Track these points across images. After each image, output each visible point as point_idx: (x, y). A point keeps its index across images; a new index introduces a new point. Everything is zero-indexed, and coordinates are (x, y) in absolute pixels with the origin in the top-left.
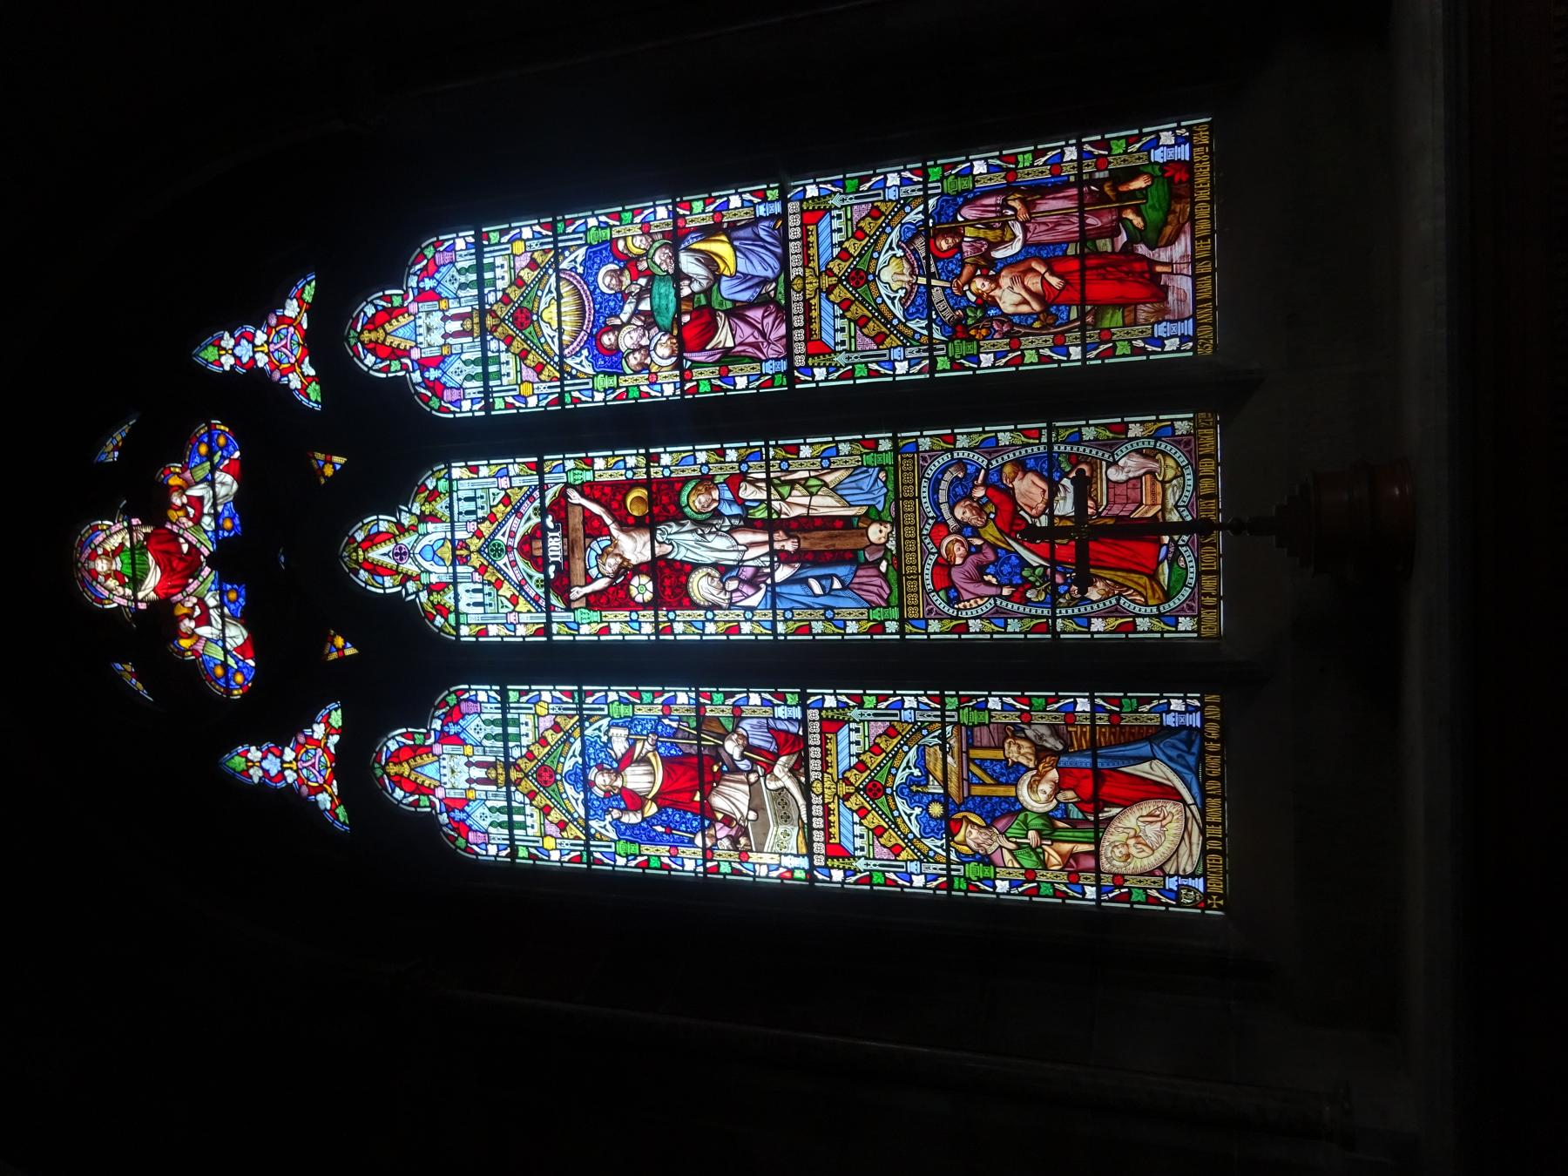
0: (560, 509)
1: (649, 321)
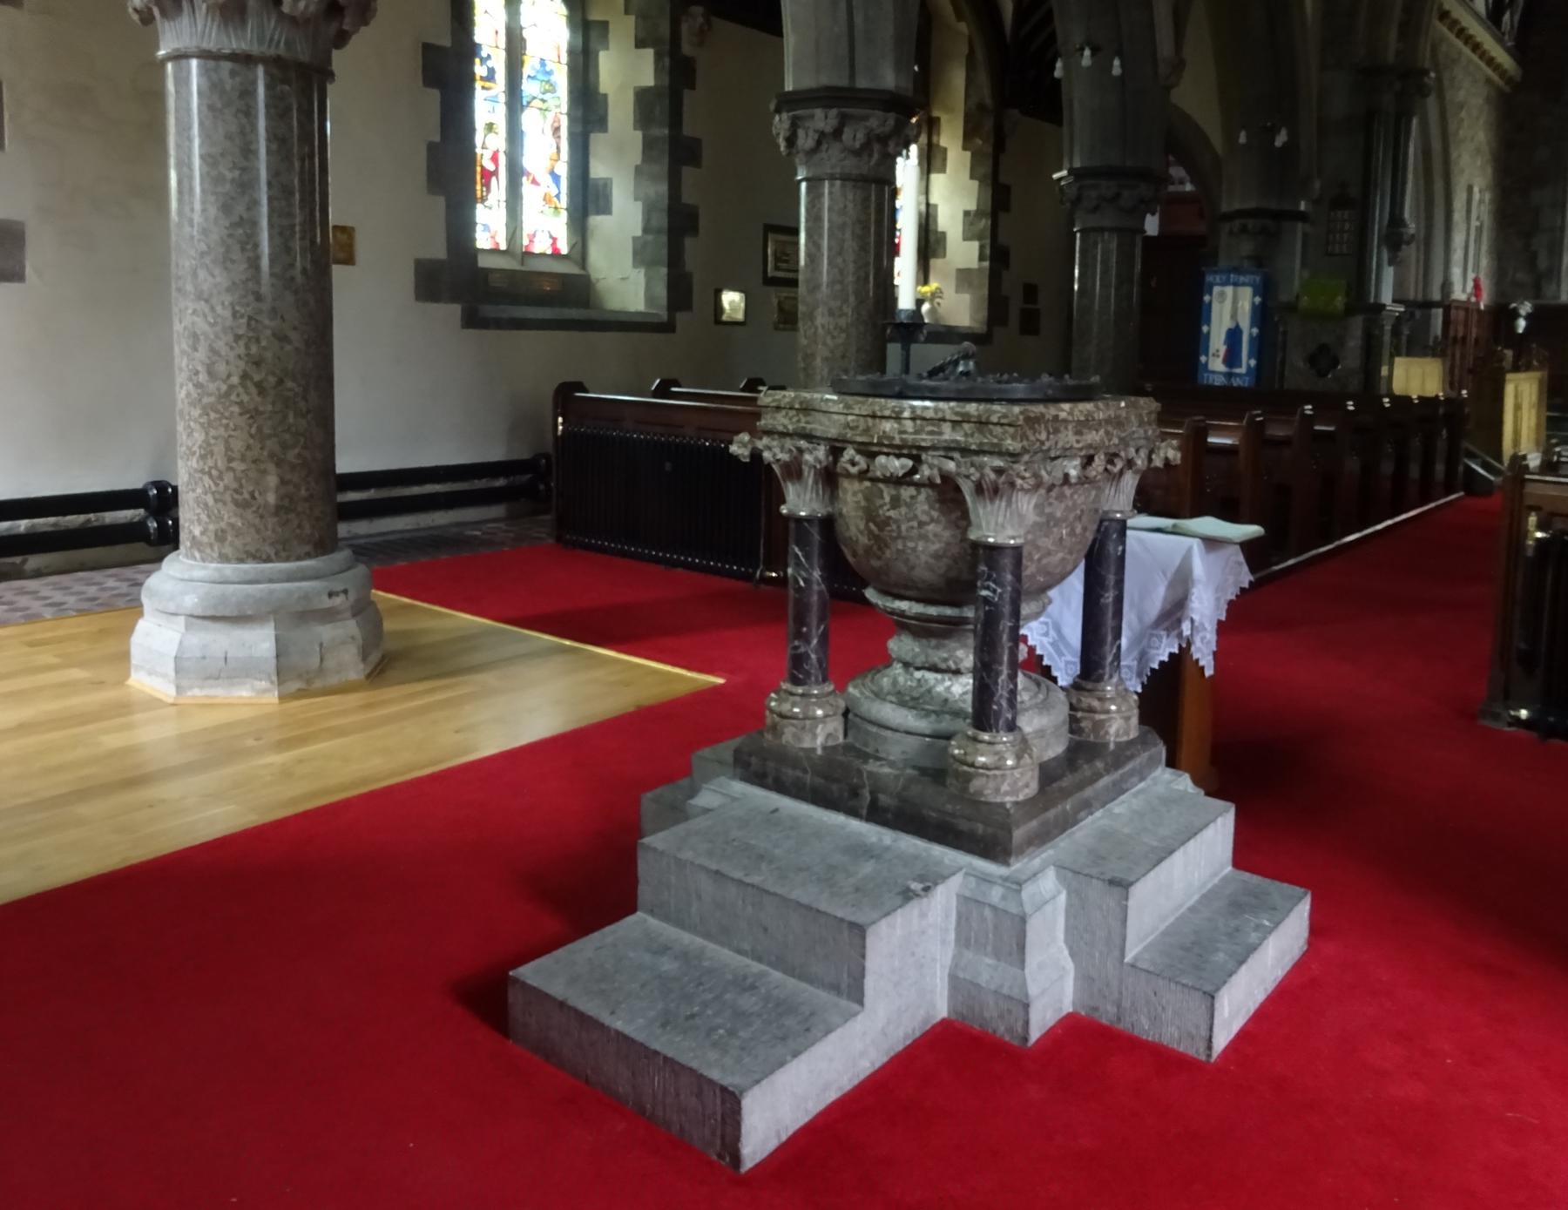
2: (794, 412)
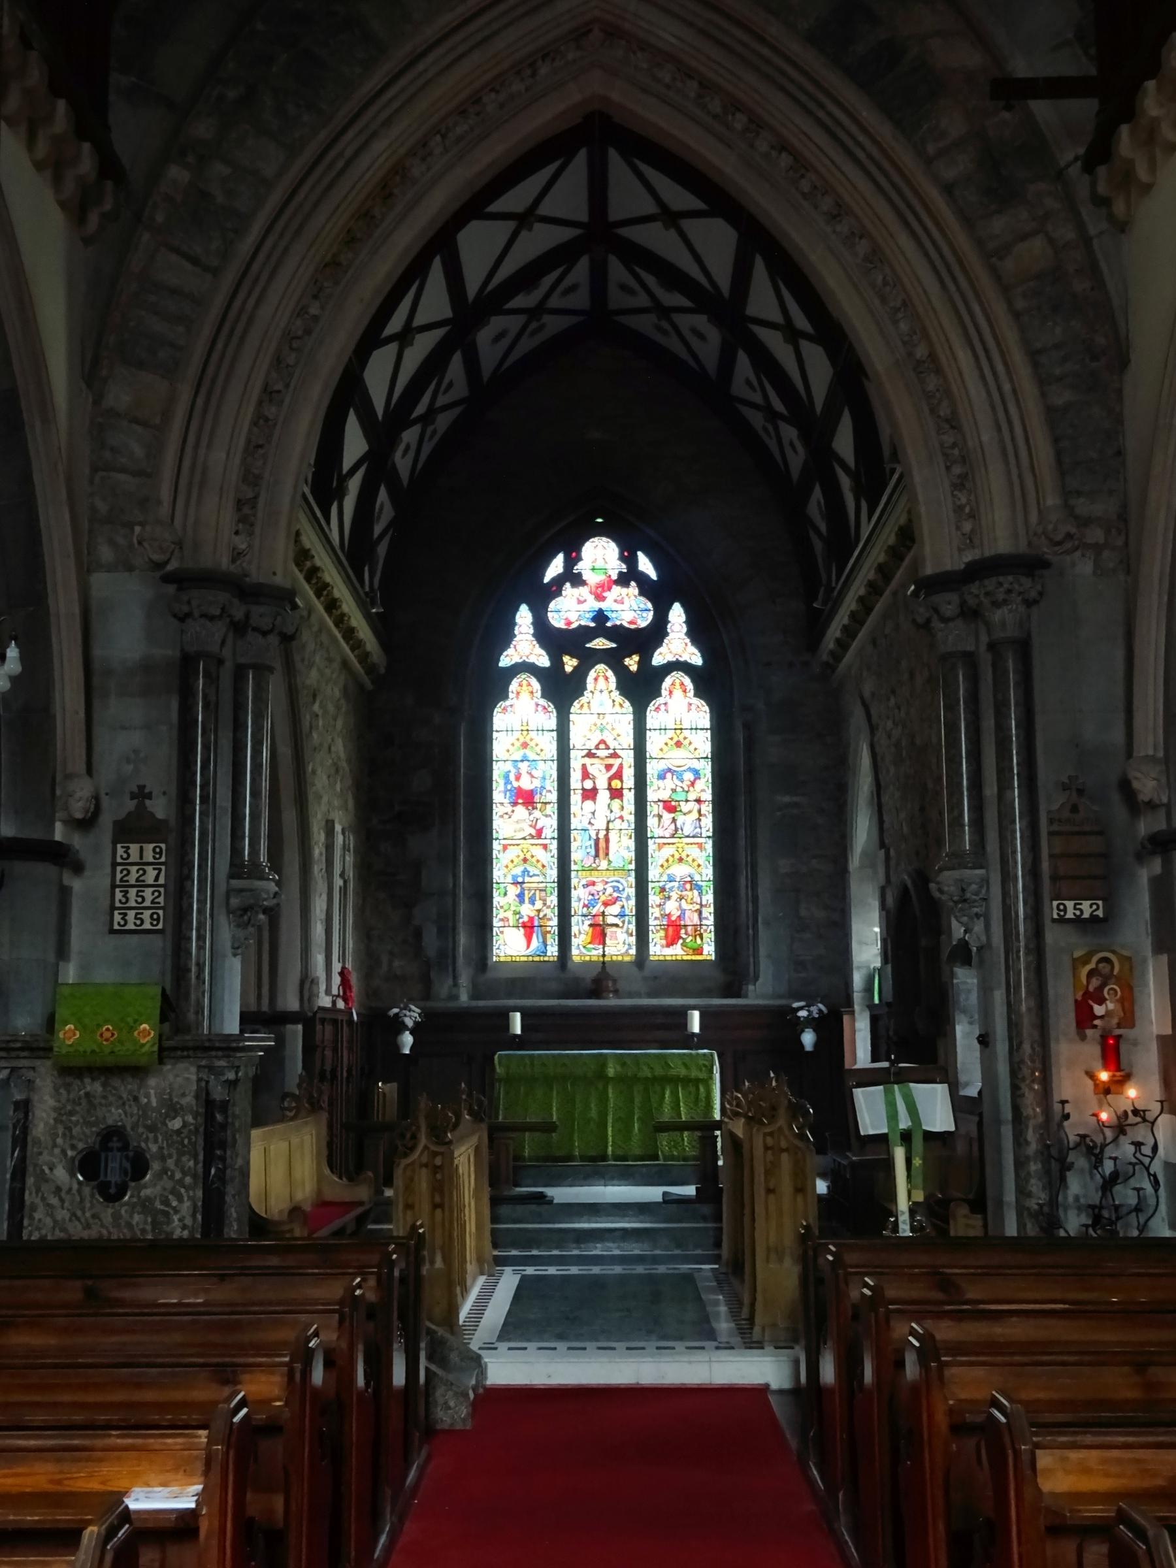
0: (615, 755)
1: (674, 791)
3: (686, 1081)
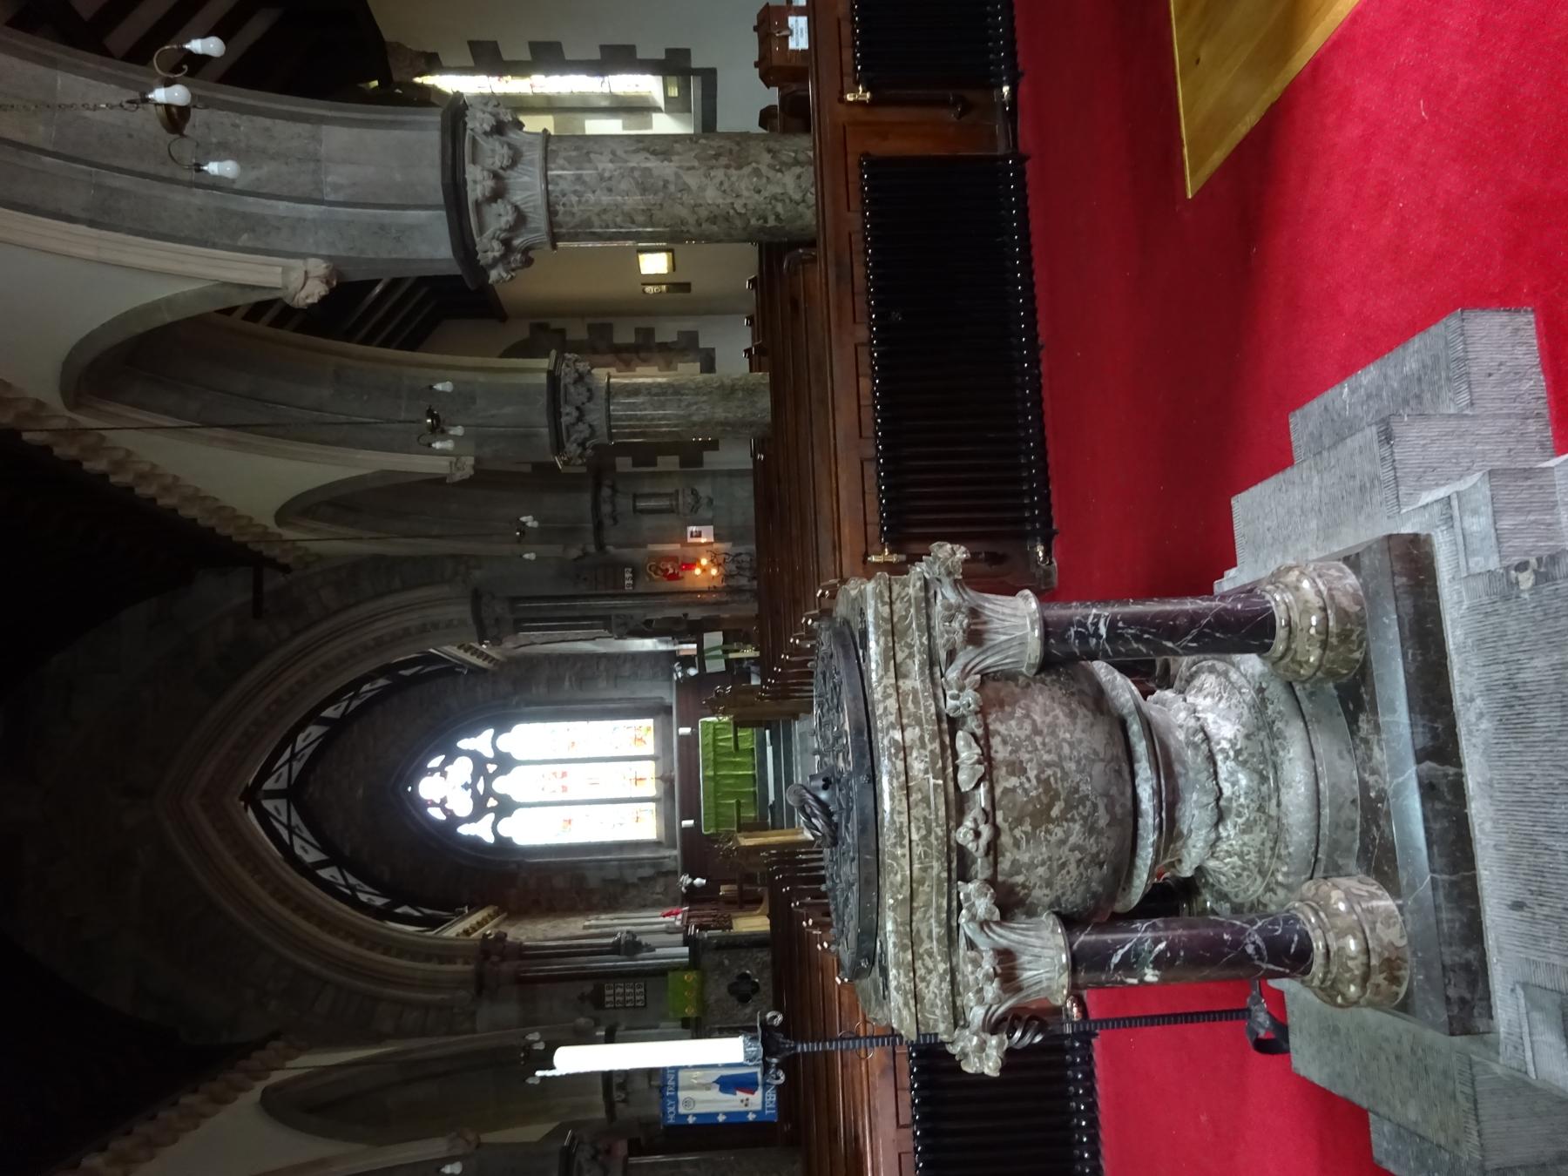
2: (918, 964)
3: (715, 734)
